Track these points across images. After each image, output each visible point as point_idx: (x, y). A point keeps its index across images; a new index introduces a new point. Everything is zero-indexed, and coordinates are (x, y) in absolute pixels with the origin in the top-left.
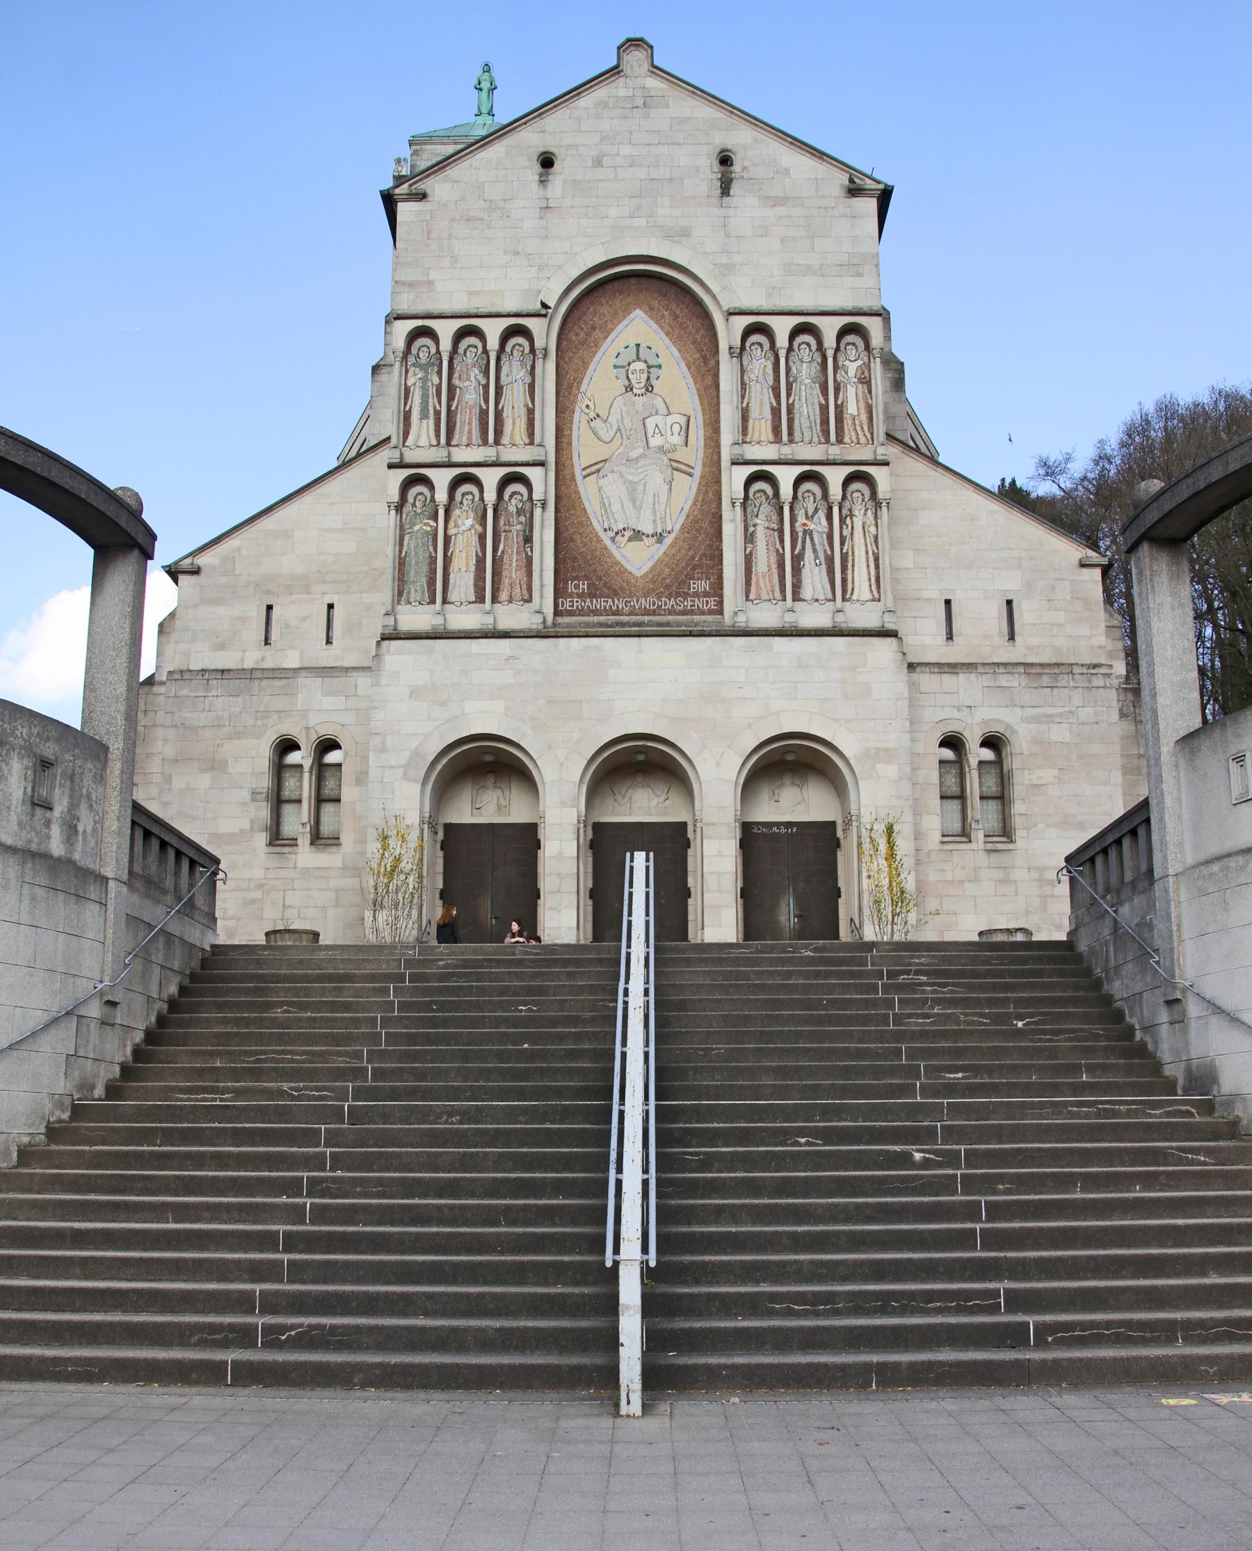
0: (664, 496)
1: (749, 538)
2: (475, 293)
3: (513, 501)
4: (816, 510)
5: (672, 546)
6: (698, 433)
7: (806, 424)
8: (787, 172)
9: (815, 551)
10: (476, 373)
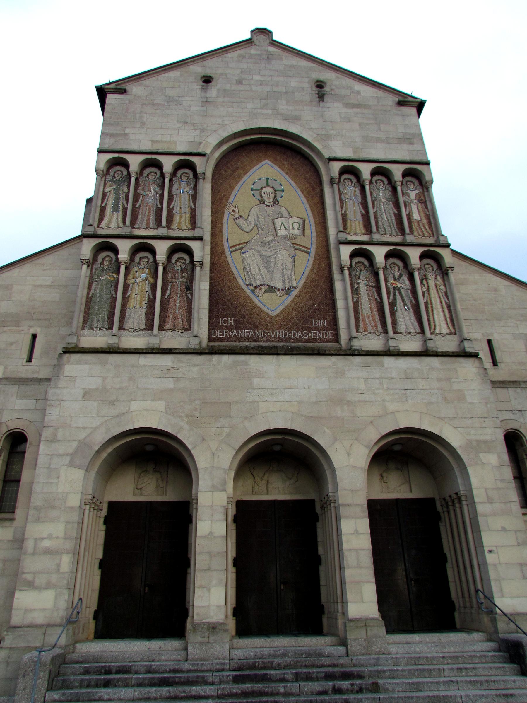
0: (289, 266)
1: (355, 291)
2: (157, 142)
3: (179, 264)
4: (401, 275)
5: (297, 296)
6: (311, 230)
7: (386, 225)
8: (359, 93)
9: (403, 301)
10: (154, 188)
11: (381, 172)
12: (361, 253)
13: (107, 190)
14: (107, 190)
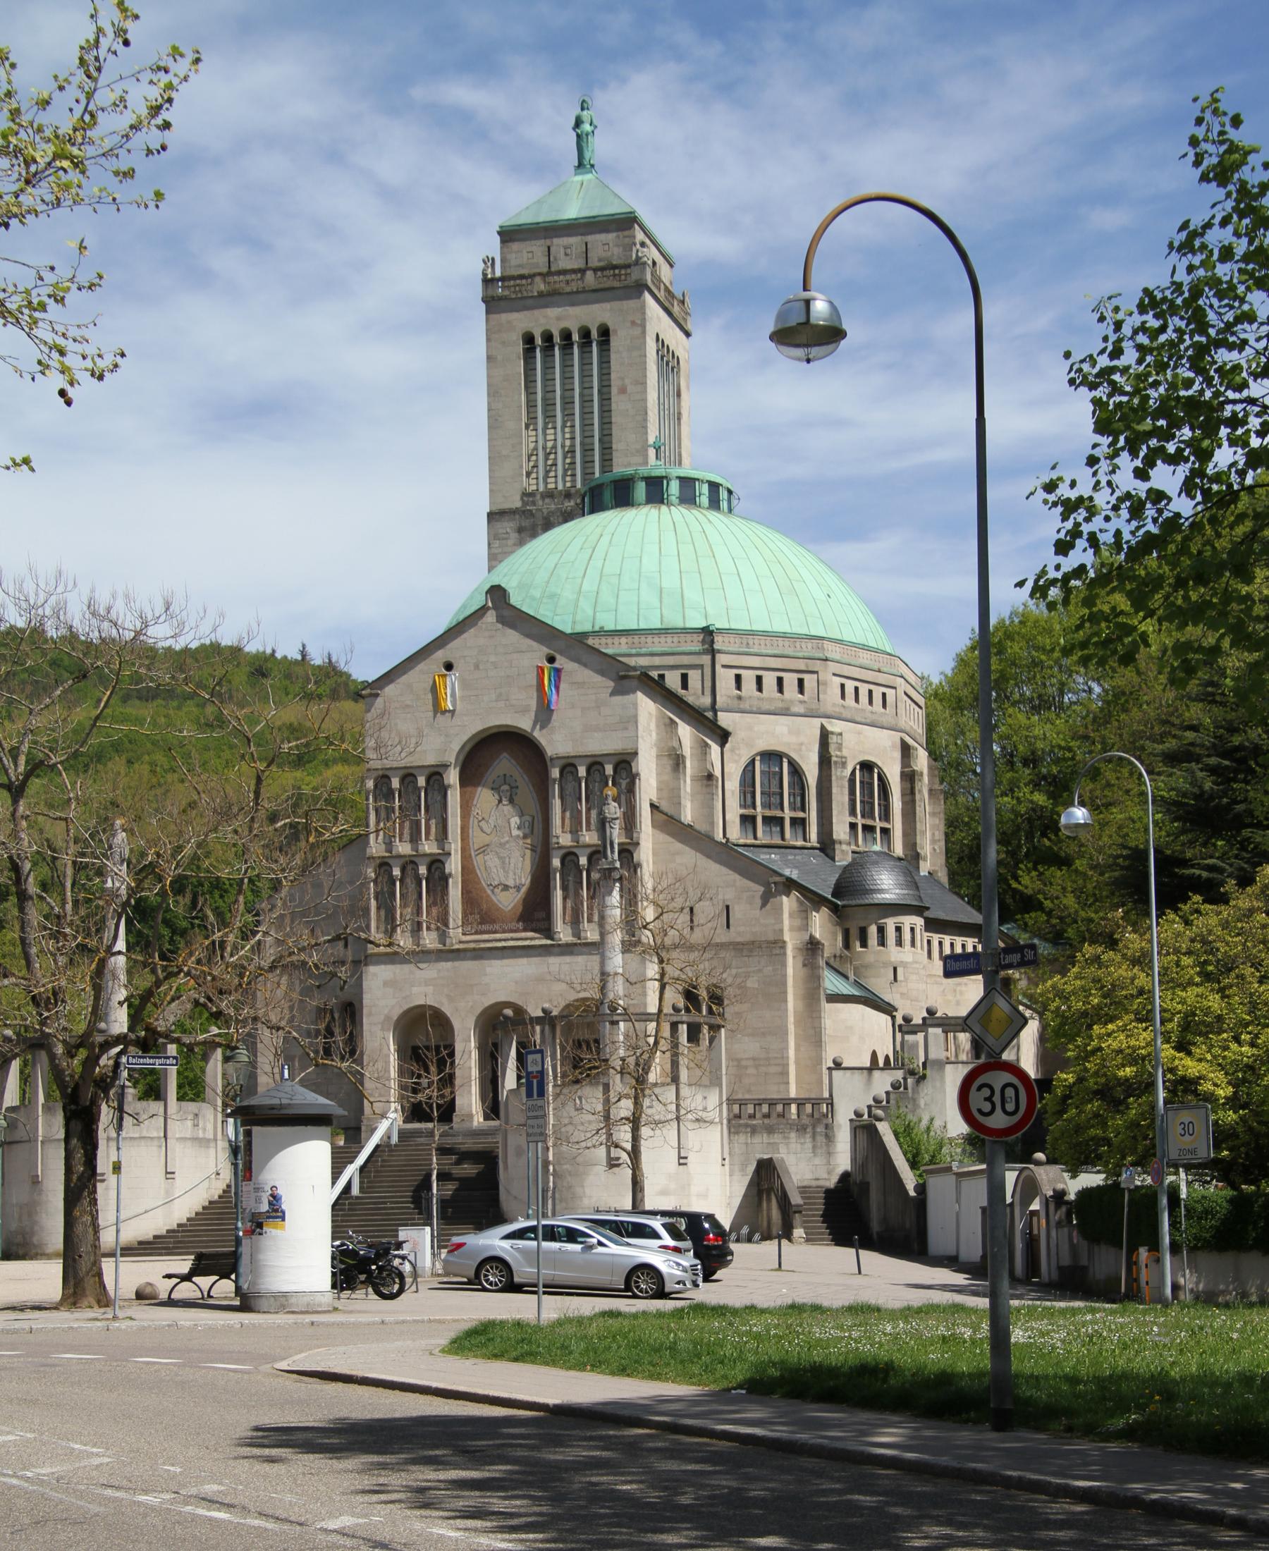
11: (595, 765)
12: (569, 857)
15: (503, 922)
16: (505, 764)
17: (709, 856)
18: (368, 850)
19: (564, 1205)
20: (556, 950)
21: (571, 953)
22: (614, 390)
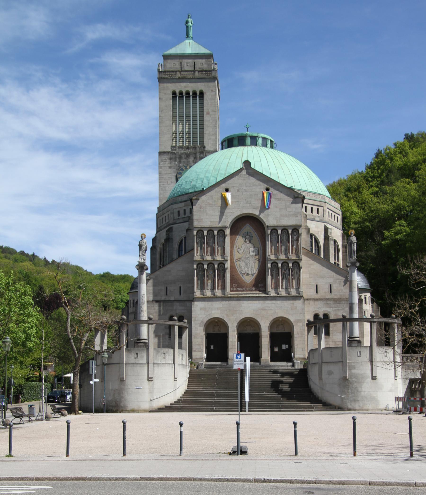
0: (253, 266)
2: (212, 222)
11: (285, 229)
12: (274, 264)
13: (198, 241)
14: (198, 241)
15: (247, 287)
16: (248, 228)
17: (323, 266)
18: (194, 258)
19: (353, 395)
20: (270, 298)
21: (276, 300)
22: (205, 113)
